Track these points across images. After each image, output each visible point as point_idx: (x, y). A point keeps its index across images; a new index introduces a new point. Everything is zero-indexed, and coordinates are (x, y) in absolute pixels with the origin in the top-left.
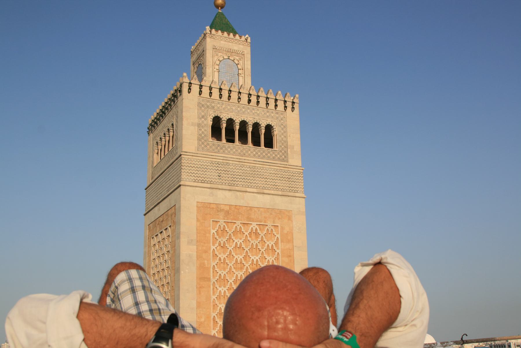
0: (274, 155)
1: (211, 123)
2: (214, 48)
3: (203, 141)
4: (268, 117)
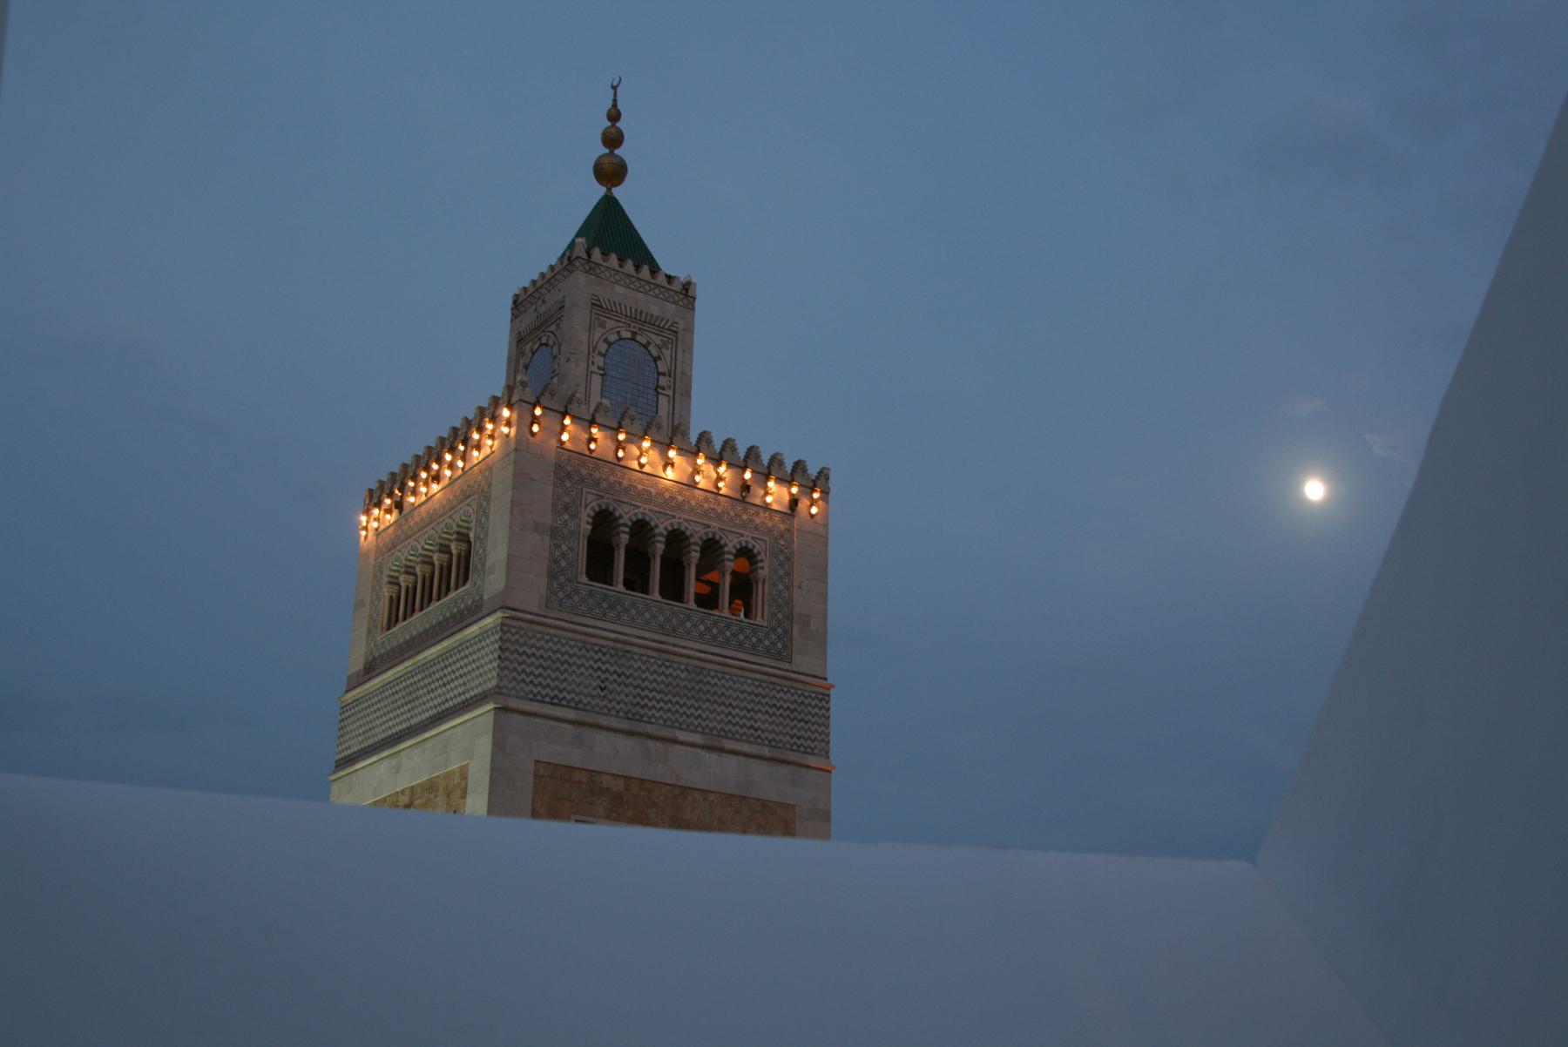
0: (754, 640)
2: (596, 305)
3: (562, 579)
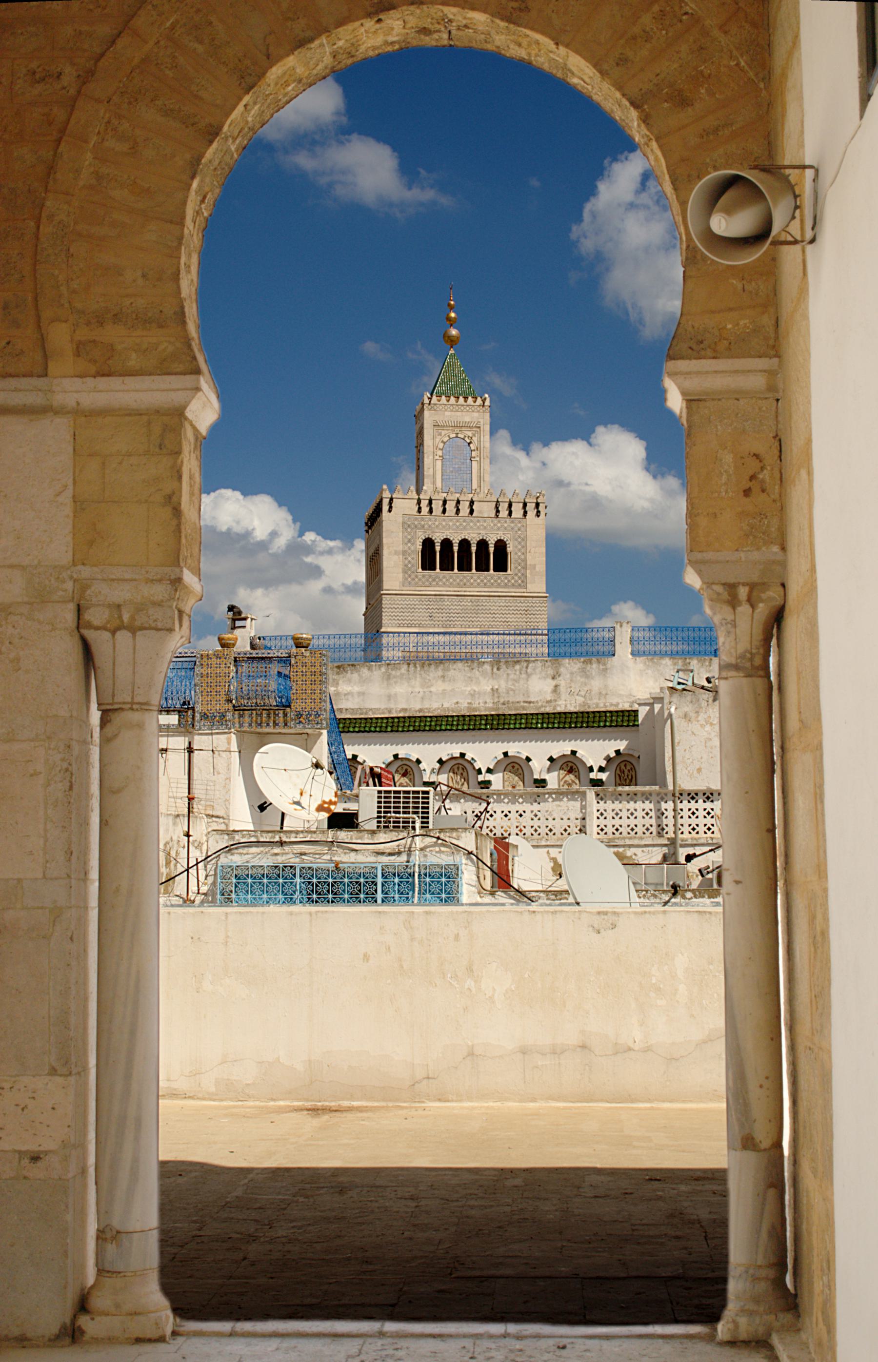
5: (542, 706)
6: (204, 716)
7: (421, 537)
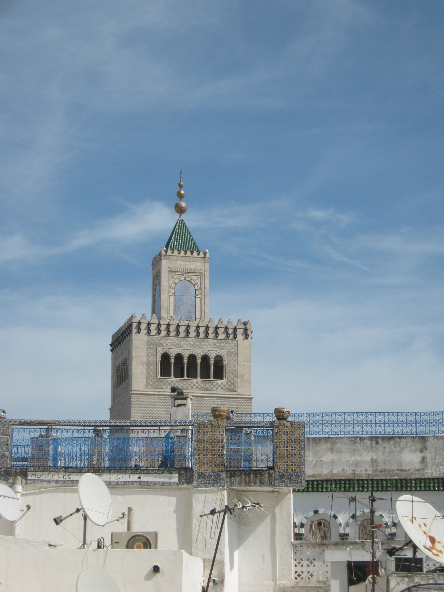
0: (222, 386)
1: (159, 359)
2: (170, 271)
3: (151, 378)
4: (217, 347)
5: (413, 474)
6: (202, 475)
7: (161, 351)
